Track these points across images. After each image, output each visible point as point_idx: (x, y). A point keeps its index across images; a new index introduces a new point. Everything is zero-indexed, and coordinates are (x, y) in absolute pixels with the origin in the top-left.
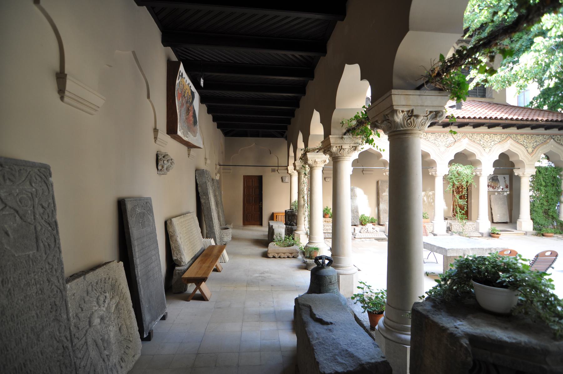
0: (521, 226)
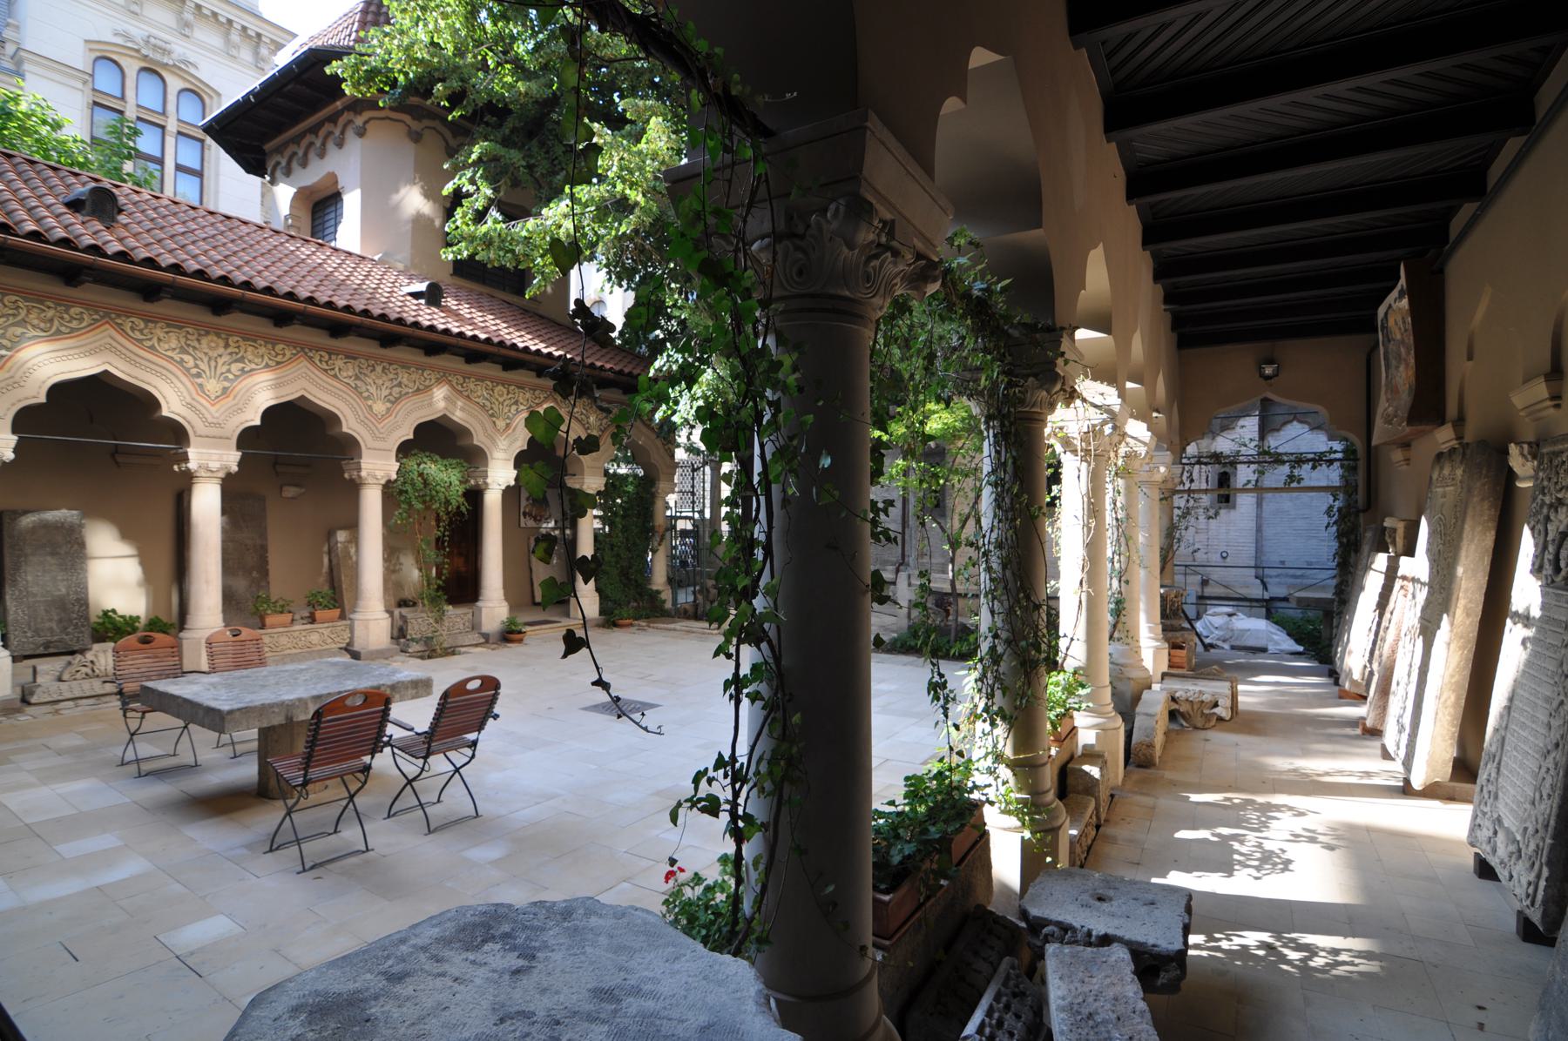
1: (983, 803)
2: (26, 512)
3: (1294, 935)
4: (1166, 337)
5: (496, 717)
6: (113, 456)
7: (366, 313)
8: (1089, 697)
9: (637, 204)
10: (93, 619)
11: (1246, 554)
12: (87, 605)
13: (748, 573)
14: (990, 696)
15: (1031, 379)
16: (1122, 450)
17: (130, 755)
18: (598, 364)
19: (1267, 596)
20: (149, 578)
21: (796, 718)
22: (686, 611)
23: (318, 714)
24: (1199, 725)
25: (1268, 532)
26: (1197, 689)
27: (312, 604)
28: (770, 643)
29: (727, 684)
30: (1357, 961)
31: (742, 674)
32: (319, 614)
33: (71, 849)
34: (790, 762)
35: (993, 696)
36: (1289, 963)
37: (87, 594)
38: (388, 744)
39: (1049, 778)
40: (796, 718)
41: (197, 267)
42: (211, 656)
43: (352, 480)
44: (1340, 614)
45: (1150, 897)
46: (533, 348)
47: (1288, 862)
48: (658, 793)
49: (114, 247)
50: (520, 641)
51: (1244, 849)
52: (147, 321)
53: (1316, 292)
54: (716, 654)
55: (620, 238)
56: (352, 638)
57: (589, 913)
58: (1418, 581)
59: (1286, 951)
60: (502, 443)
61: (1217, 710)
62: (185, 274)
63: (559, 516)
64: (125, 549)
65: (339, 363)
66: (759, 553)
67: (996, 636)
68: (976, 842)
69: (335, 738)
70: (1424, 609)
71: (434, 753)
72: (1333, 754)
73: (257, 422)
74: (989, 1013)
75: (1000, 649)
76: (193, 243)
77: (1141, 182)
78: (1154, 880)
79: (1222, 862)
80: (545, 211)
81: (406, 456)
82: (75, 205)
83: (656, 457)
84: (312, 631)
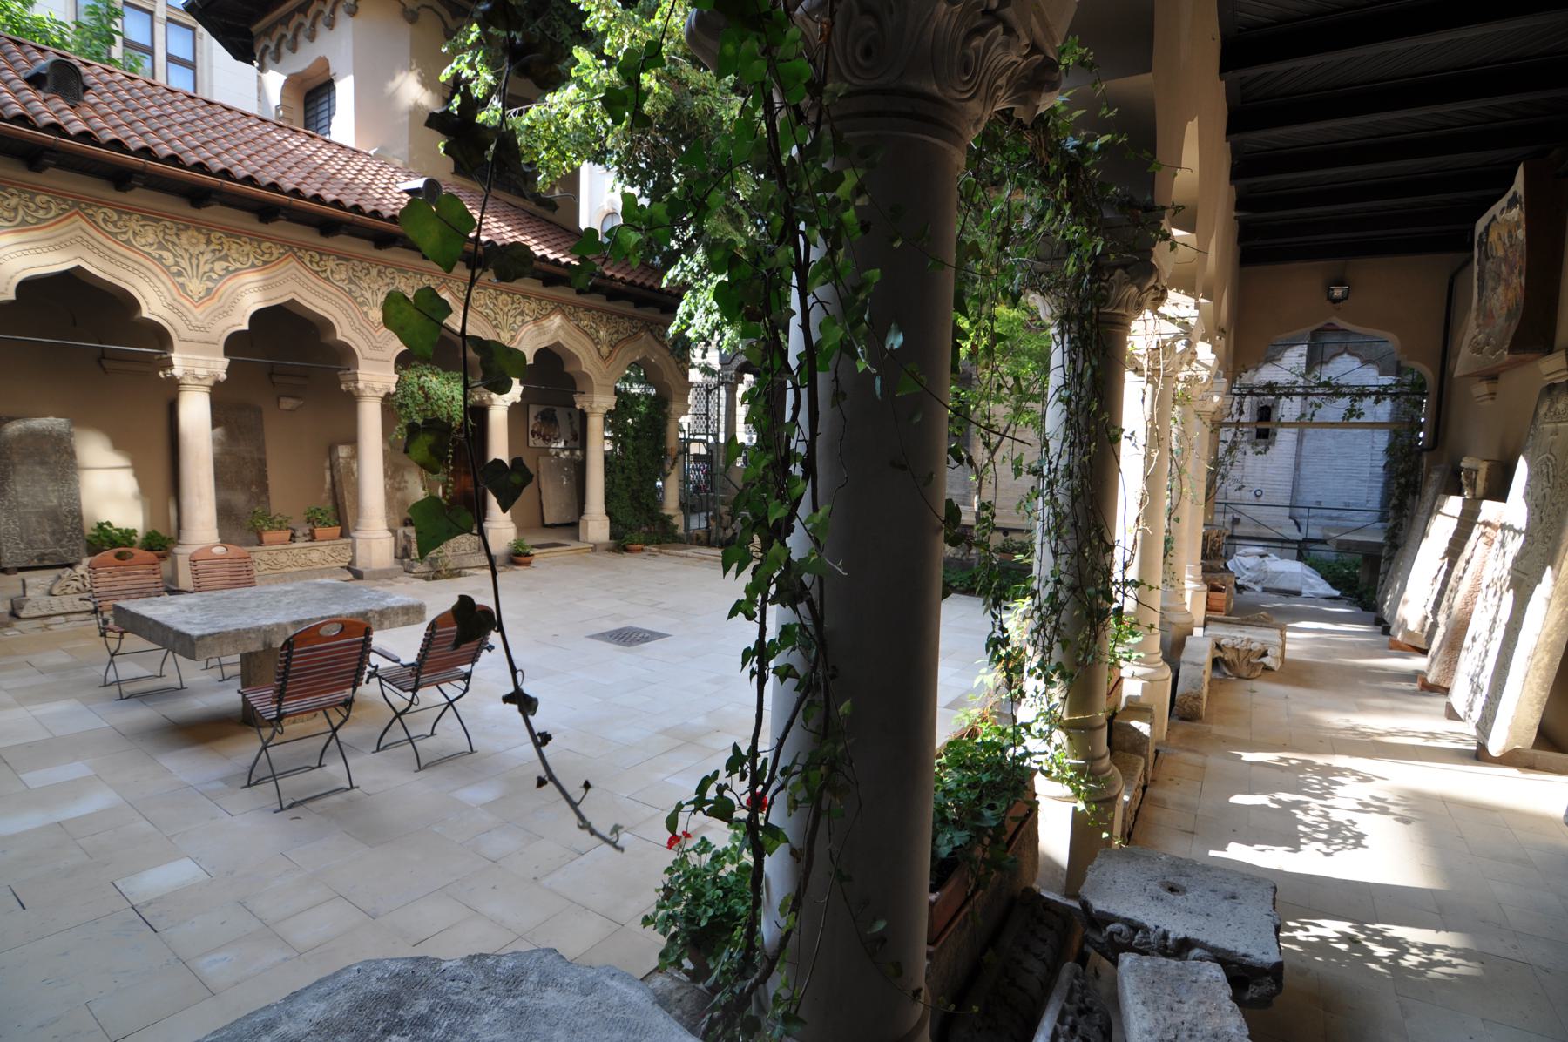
1: (1035, 771)
2: (11, 419)
3: (1378, 926)
6: (99, 361)
7: (356, 208)
8: (1138, 647)
9: (650, 89)
10: (88, 532)
11: (1282, 493)
12: (80, 516)
13: (781, 497)
14: (1047, 650)
15: (1119, 272)
17: (111, 677)
19: (1299, 537)
20: (145, 489)
21: (845, 708)
22: (698, 538)
23: (288, 644)
24: (1244, 674)
25: (1306, 471)
26: (1246, 636)
27: (313, 520)
28: (811, 604)
29: (747, 655)
30: (1455, 961)
31: (767, 640)
32: (319, 531)
33: (36, 778)
34: (832, 768)
35: (1050, 649)
36: (1377, 960)
37: (80, 506)
38: (372, 675)
40: (845, 708)
41: (170, 152)
42: (195, 574)
43: (349, 393)
44: (1390, 559)
45: (1229, 888)
47: (1359, 837)
48: (665, 732)
49: (77, 127)
50: (528, 564)
51: (1308, 819)
52: (120, 213)
53: (1407, 200)
54: (733, 613)
56: (354, 557)
57: (546, 981)
58: (1511, 528)
59: (1372, 946)
61: (1266, 660)
62: (156, 159)
63: (569, 436)
64: (118, 460)
65: (331, 264)
66: (797, 469)
68: (1027, 816)
69: (309, 670)
70: (1516, 560)
71: (422, 686)
72: (1391, 711)
73: (246, 327)
75: (1061, 596)
76: (169, 127)
78: (1212, 853)
80: (549, 97)
81: (405, 368)
82: (36, 81)
83: (669, 377)
84: (310, 549)
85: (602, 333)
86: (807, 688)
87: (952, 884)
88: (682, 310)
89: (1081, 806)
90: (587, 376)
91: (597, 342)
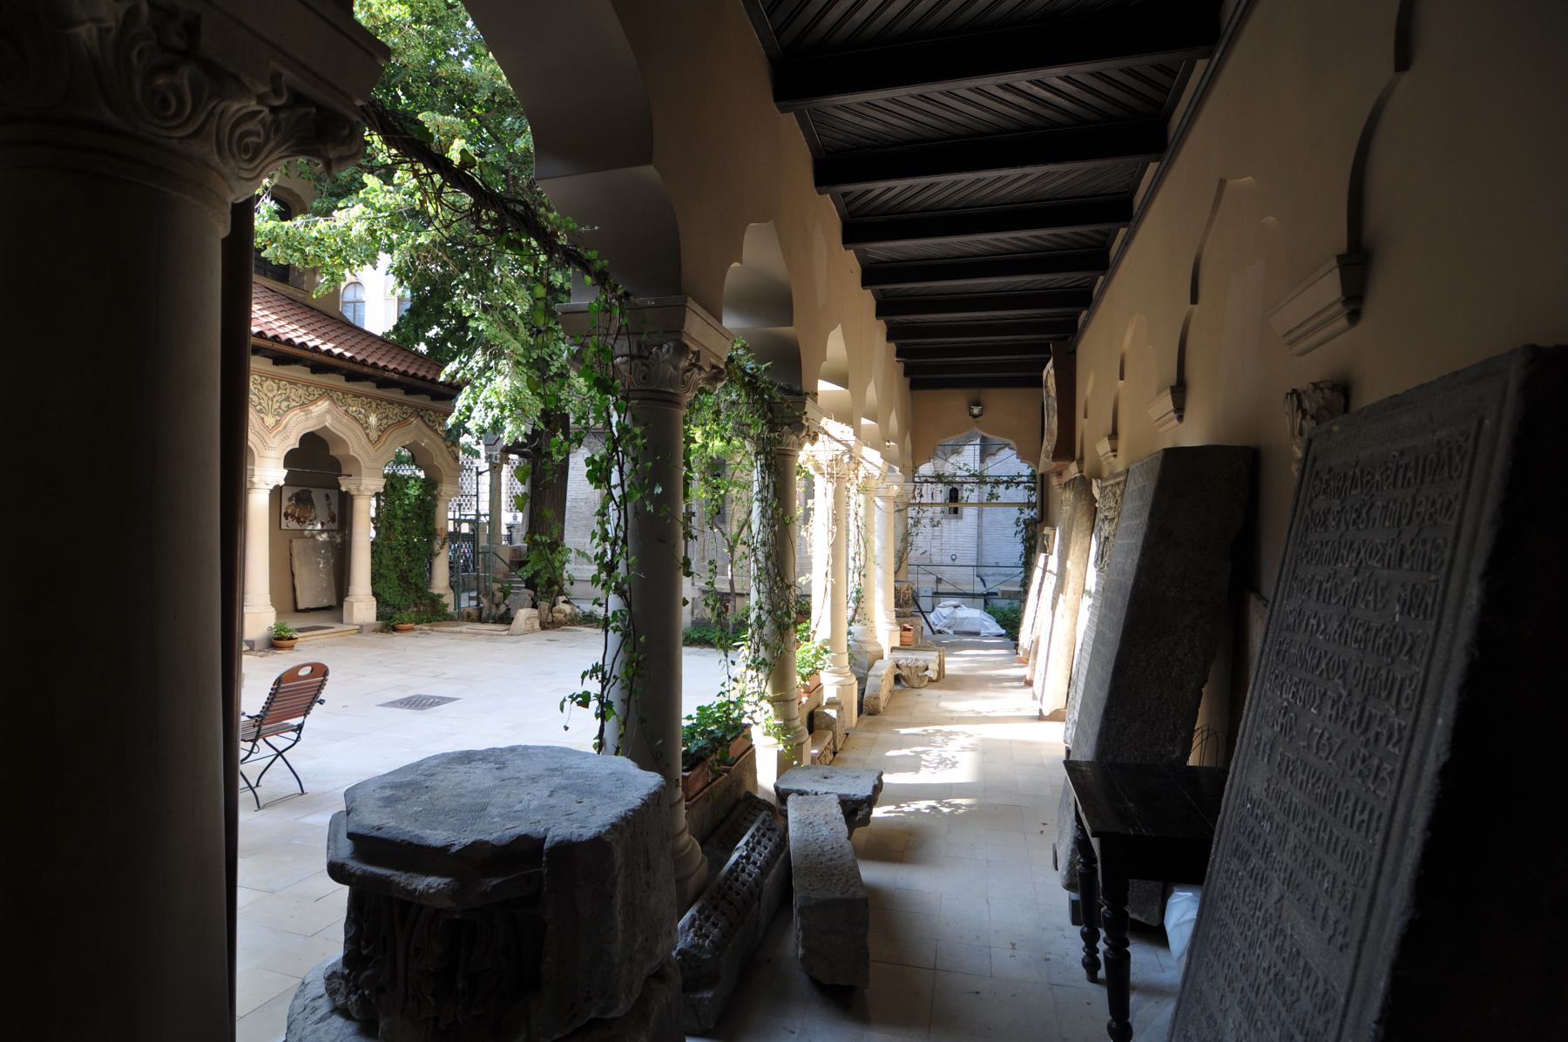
0: (351, 613)
4: (898, 382)
5: (322, 702)
11: (969, 557)
16: (862, 473)
18: (381, 364)
21: (642, 639)
22: (469, 615)
25: (986, 538)
39: (800, 723)
46: (311, 344)
50: (291, 647)
55: (417, 248)
60: (274, 441)
63: (326, 519)
67: (761, 608)
74: (753, 836)
77: (872, 275)
79: (914, 765)
85: (373, 420)
86: (625, 636)
87: (698, 770)
88: (461, 402)
89: (781, 747)
90: (355, 460)
91: (365, 427)
